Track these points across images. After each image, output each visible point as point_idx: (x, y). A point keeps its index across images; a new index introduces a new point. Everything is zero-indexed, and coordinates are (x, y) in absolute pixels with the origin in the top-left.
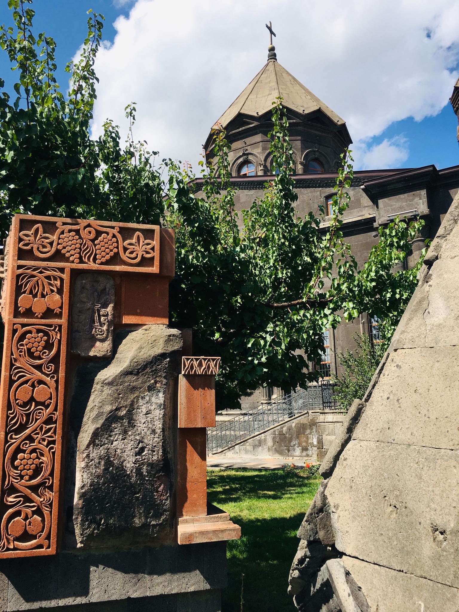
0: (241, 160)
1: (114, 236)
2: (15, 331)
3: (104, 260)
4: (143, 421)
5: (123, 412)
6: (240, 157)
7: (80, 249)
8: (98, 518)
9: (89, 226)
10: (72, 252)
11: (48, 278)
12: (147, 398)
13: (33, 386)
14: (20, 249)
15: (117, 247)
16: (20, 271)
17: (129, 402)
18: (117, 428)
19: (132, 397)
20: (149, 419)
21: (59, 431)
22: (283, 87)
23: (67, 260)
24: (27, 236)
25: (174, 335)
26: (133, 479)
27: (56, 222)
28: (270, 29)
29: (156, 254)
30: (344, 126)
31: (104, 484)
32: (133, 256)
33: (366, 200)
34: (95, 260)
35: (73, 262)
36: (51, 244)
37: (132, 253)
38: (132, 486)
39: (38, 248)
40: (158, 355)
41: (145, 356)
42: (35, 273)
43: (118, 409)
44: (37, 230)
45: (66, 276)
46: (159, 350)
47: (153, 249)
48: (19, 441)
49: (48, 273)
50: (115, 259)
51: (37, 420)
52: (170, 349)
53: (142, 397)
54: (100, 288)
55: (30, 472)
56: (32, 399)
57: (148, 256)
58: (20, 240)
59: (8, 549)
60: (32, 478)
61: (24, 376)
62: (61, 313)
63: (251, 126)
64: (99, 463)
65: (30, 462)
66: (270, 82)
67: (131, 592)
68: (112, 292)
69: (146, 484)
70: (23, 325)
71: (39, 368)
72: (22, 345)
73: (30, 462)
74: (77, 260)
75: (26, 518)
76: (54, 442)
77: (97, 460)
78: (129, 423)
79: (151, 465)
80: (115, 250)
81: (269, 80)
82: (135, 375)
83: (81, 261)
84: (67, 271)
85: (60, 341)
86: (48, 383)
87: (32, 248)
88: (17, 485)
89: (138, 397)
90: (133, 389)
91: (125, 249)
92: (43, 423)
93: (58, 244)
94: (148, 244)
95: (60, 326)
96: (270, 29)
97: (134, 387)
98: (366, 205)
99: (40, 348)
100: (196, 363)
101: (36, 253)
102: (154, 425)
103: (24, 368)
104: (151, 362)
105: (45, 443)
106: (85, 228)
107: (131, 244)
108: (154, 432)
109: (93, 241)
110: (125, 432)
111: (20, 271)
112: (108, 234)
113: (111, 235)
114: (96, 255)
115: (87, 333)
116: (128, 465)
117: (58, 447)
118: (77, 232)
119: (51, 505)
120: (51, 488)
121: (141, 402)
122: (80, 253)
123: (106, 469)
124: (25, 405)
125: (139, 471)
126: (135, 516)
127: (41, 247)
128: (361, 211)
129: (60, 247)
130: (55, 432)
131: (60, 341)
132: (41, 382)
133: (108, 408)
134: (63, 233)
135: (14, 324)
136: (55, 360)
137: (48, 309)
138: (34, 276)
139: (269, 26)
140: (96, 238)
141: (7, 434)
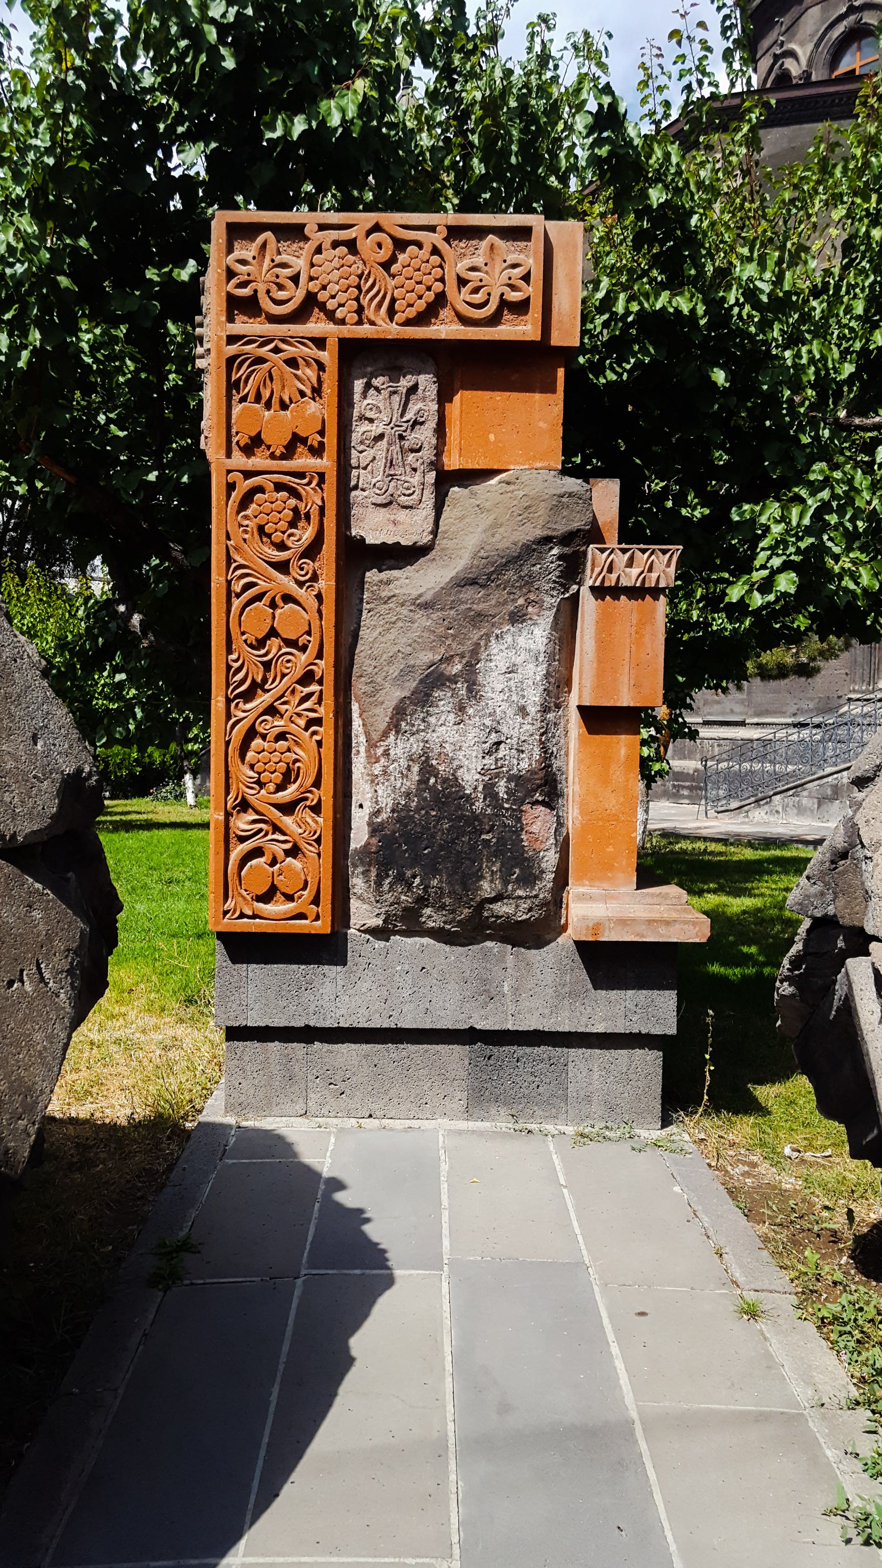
0: (840, 29)
1: (435, 251)
3: (411, 313)
4: (499, 687)
5: (457, 668)
7: (358, 287)
8: (409, 873)
9: (377, 228)
10: (342, 297)
11: (292, 362)
12: (509, 639)
13: (273, 605)
14: (230, 297)
15: (442, 280)
16: (233, 349)
17: (468, 646)
18: (444, 702)
19: (475, 635)
20: (512, 683)
21: (329, 700)
24: (243, 262)
25: (571, 495)
26: (479, 805)
27: (304, 225)
29: (533, 291)
31: (418, 809)
32: (479, 298)
34: (391, 312)
35: (342, 322)
36: (295, 279)
37: (476, 290)
38: (475, 817)
39: (268, 292)
40: (534, 542)
41: (506, 544)
42: (264, 351)
43: (447, 660)
45: (328, 357)
46: (533, 532)
47: (526, 278)
48: (252, 716)
49: (290, 351)
51: (284, 676)
52: (562, 528)
53: (497, 636)
55: (278, 777)
56: (273, 632)
57: (514, 296)
58: (231, 274)
59: (242, 916)
60: (280, 788)
61: (253, 585)
62: (322, 444)
64: (409, 768)
65: (276, 757)
67: (476, 1016)
69: (504, 816)
70: (248, 474)
71: (282, 567)
72: (246, 517)
73: (276, 757)
75: (274, 862)
76: (318, 722)
77: (403, 763)
78: (470, 690)
79: (517, 779)
80: (438, 287)
82: (483, 586)
84: (332, 344)
85: (322, 509)
86: (301, 600)
87: (256, 291)
88: (252, 800)
89: (488, 636)
90: (478, 619)
91: (462, 282)
92: (298, 682)
93: (311, 279)
94: (514, 266)
95: (322, 476)
97: (479, 614)
99: (283, 525)
102: (523, 697)
103: (251, 565)
104: (518, 557)
105: (302, 722)
106: (369, 233)
107: (473, 269)
108: (522, 711)
109: (386, 265)
110: (461, 709)
111: (233, 349)
112: (419, 245)
113: (427, 248)
114: (393, 300)
115: (378, 492)
116: (467, 777)
117: (326, 732)
118: (351, 246)
119: (318, 841)
120: (316, 809)
121: (495, 647)
122: (357, 299)
123: (423, 781)
124: (261, 643)
125: (489, 790)
126: (482, 877)
127: (274, 288)
129: (314, 286)
130: (319, 702)
131: (322, 509)
132: (288, 598)
133: (426, 657)
134: (319, 250)
135: (229, 472)
136: (312, 551)
137: (295, 435)
138: (261, 360)
140: (393, 260)
141: (228, 701)
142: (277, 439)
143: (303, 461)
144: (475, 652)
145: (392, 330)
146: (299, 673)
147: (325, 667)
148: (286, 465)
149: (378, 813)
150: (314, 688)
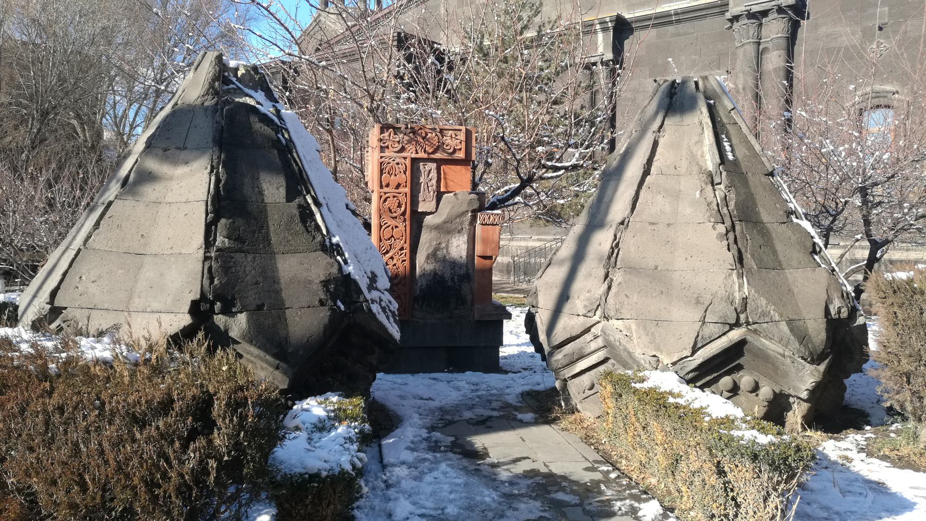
2: (381, 197)
11: (398, 164)
16: (382, 160)
21: (408, 255)
45: (408, 162)
46: (464, 208)
49: (398, 160)
56: (392, 236)
57: (458, 147)
70: (385, 193)
74: (414, 152)
76: (405, 261)
100: (487, 217)
120: (404, 285)
125: (453, 279)
133: (434, 243)
136: (404, 214)
138: (389, 163)
142: (393, 184)
143: (401, 190)
144: (448, 241)
146: (400, 247)
147: (407, 246)
148: (397, 191)
149: (422, 286)
150: (404, 251)
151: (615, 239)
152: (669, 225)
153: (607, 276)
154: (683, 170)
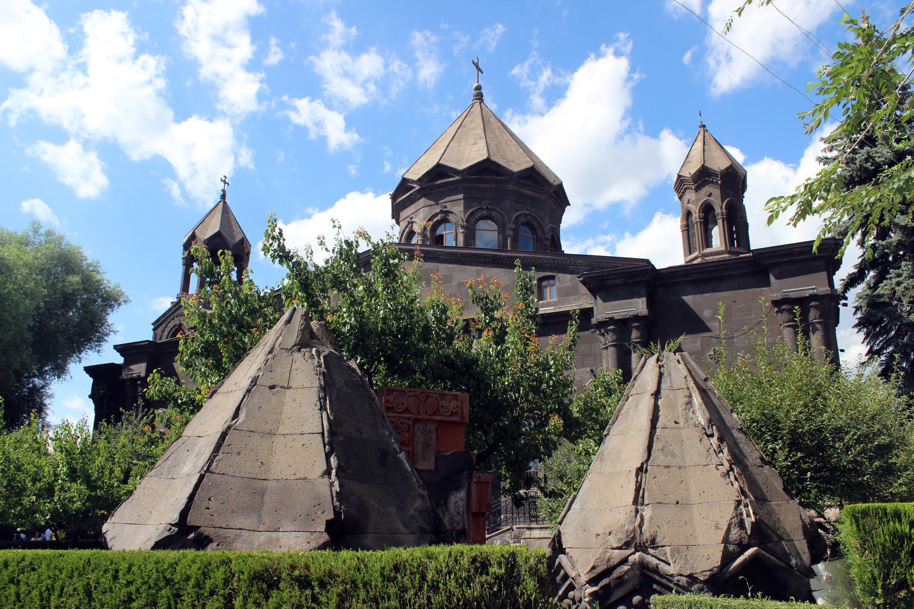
6: (436, 215)
11: (402, 423)
22: (491, 136)
23: (411, 413)
28: (477, 65)
30: (561, 186)
33: (583, 289)
34: (426, 412)
44: (396, 396)
45: (410, 422)
50: (436, 412)
54: (428, 429)
57: (455, 411)
63: (452, 179)
66: (475, 128)
68: (434, 432)
81: (473, 126)
83: (419, 413)
96: (477, 65)
98: (584, 292)
101: (396, 409)
108: (459, 513)
118: (416, 396)
128: (579, 299)
129: (408, 405)
139: (476, 61)
145: (427, 417)
151: (637, 482)
152: (680, 468)
153: (637, 511)
154: (682, 424)
